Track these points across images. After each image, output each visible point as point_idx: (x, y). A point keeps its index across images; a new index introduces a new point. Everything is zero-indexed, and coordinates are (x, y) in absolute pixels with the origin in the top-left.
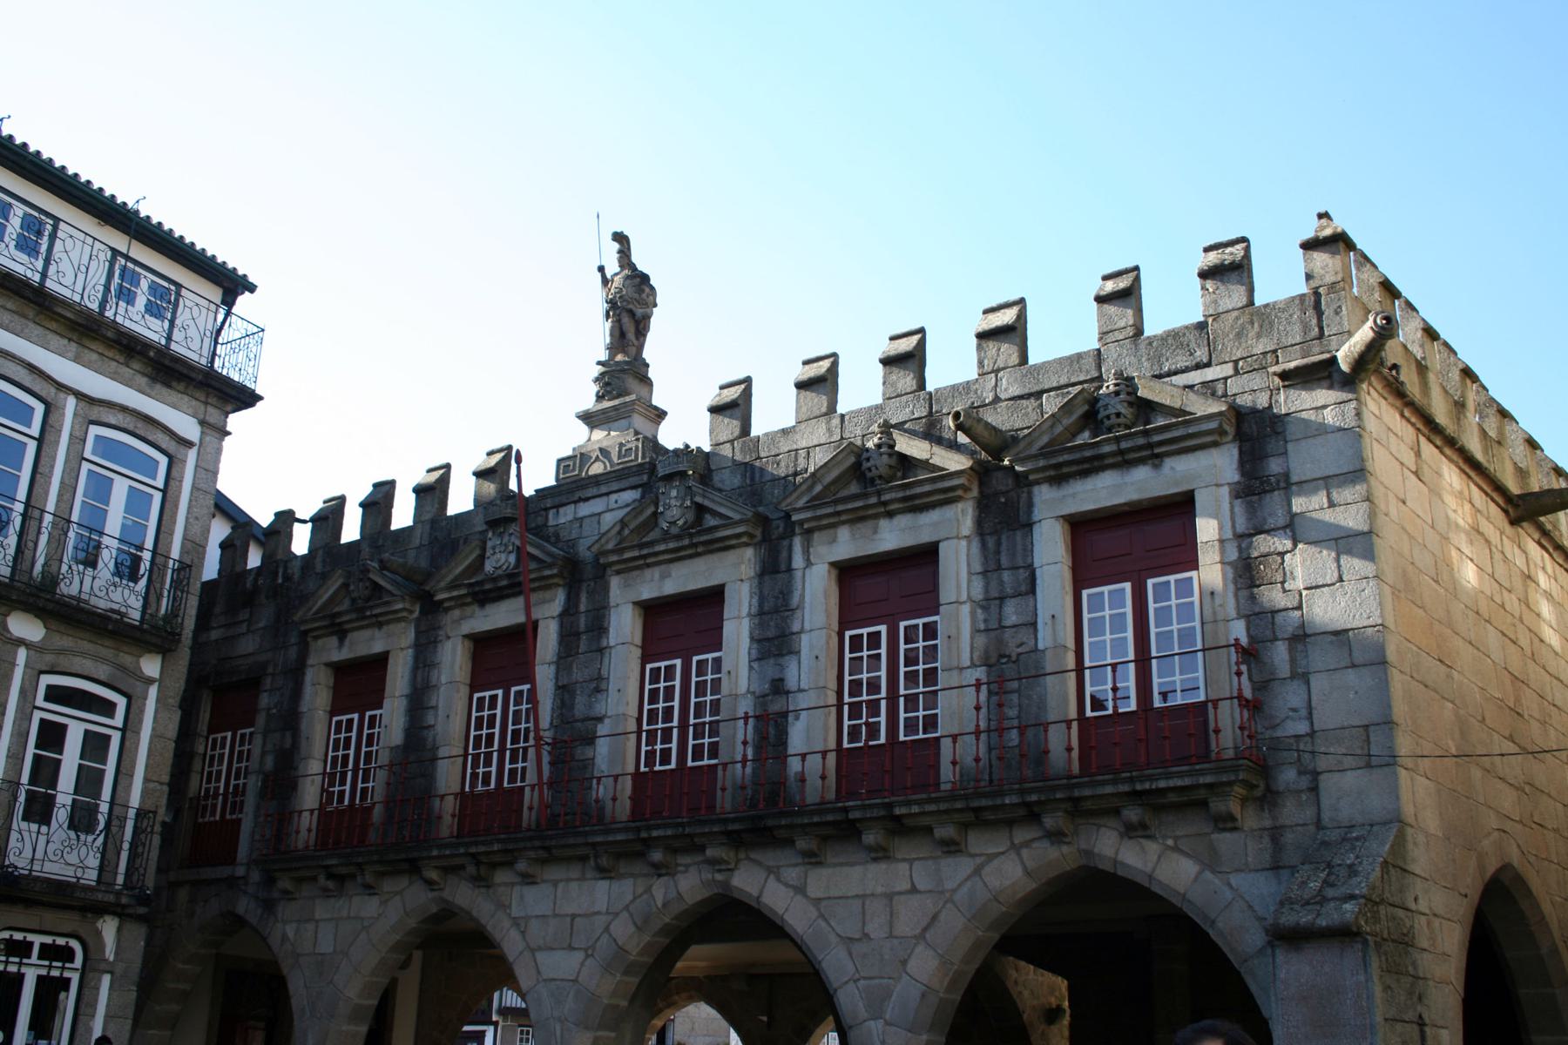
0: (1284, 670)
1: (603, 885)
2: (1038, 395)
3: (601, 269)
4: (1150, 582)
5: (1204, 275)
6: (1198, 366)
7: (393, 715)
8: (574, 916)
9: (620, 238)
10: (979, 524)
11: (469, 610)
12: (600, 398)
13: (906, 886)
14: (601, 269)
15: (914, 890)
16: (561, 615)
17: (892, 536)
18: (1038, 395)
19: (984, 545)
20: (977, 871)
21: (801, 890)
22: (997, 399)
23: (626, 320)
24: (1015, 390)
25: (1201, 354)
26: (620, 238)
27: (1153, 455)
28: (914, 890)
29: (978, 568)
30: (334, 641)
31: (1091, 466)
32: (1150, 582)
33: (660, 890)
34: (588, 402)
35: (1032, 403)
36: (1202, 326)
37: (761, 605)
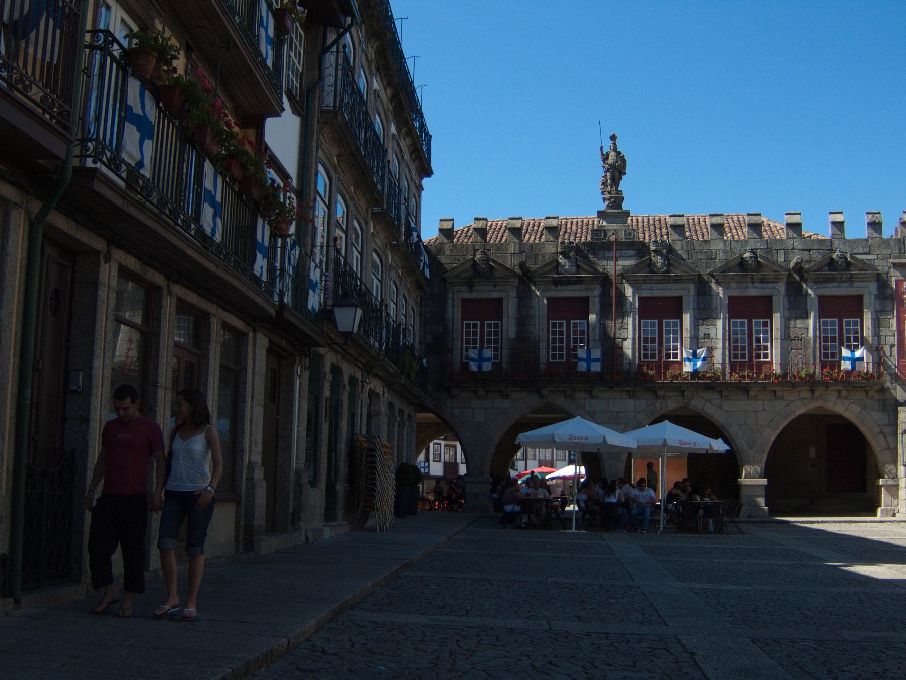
0: (888, 354)
1: (631, 401)
2: (809, 251)
3: (602, 148)
4: (844, 320)
5: (869, 224)
6: (865, 254)
7: (509, 327)
8: (618, 412)
9: (613, 138)
10: (787, 291)
11: (549, 287)
12: (608, 206)
13: (761, 408)
14: (602, 148)
15: (764, 410)
16: (600, 296)
17: (754, 291)
18: (809, 251)
19: (789, 301)
20: (788, 405)
21: (720, 407)
22: (793, 249)
23: (617, 174)
24: (799, 247)
25: (866, 250)
26: (613, 138)
27: (851, 279)
28: (764, 410)
29: (787, 306)
30: (465, 288)
31: (828, 280)
32: (844, 320)
33: (658, 404)
34: (602, 206)
35: (807, 253)
36: (867, 240)
37: (698, 306)
